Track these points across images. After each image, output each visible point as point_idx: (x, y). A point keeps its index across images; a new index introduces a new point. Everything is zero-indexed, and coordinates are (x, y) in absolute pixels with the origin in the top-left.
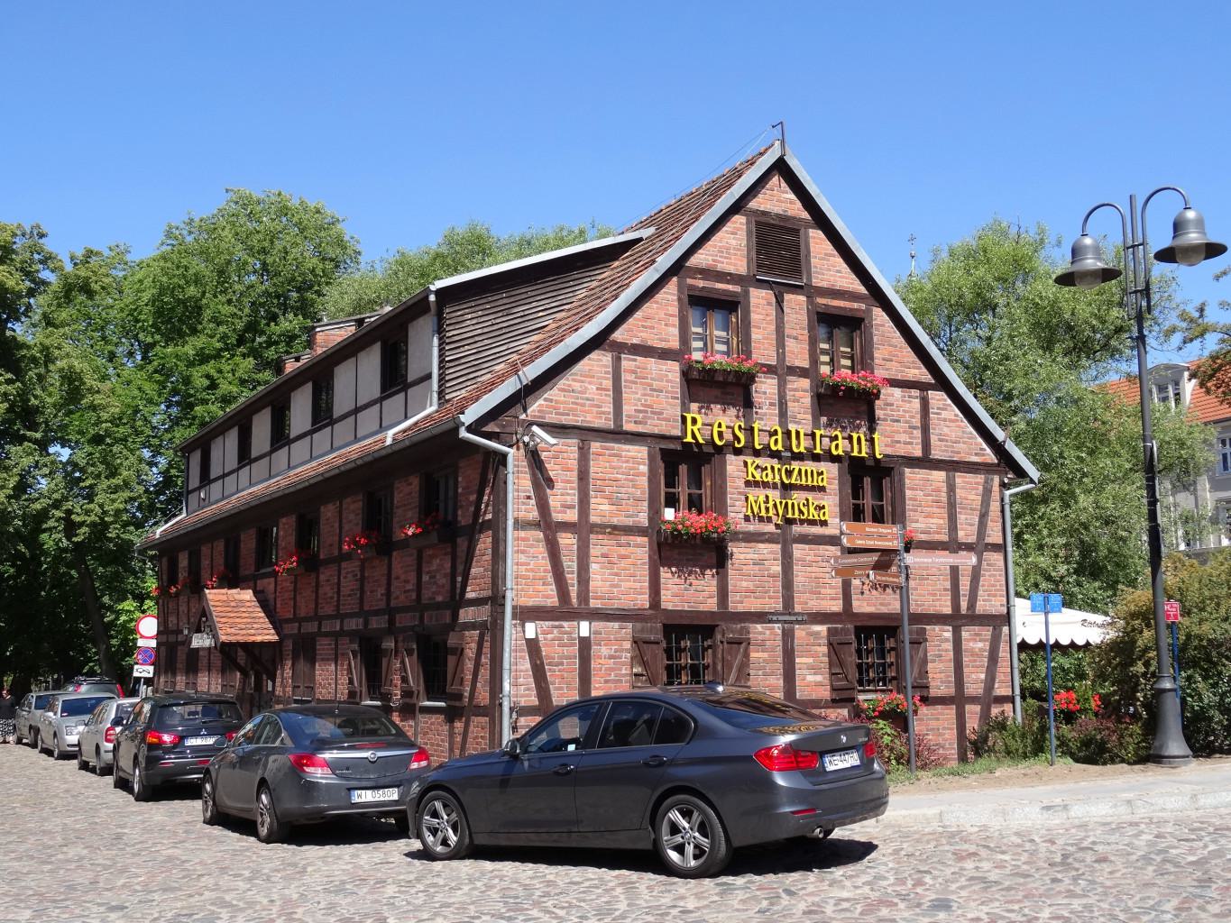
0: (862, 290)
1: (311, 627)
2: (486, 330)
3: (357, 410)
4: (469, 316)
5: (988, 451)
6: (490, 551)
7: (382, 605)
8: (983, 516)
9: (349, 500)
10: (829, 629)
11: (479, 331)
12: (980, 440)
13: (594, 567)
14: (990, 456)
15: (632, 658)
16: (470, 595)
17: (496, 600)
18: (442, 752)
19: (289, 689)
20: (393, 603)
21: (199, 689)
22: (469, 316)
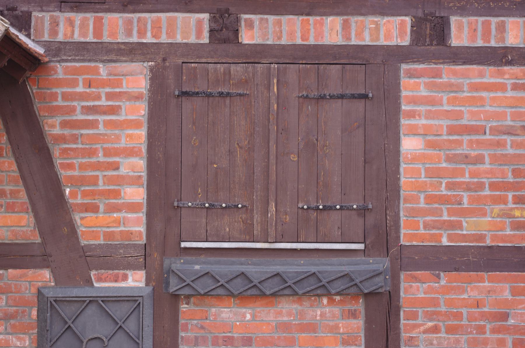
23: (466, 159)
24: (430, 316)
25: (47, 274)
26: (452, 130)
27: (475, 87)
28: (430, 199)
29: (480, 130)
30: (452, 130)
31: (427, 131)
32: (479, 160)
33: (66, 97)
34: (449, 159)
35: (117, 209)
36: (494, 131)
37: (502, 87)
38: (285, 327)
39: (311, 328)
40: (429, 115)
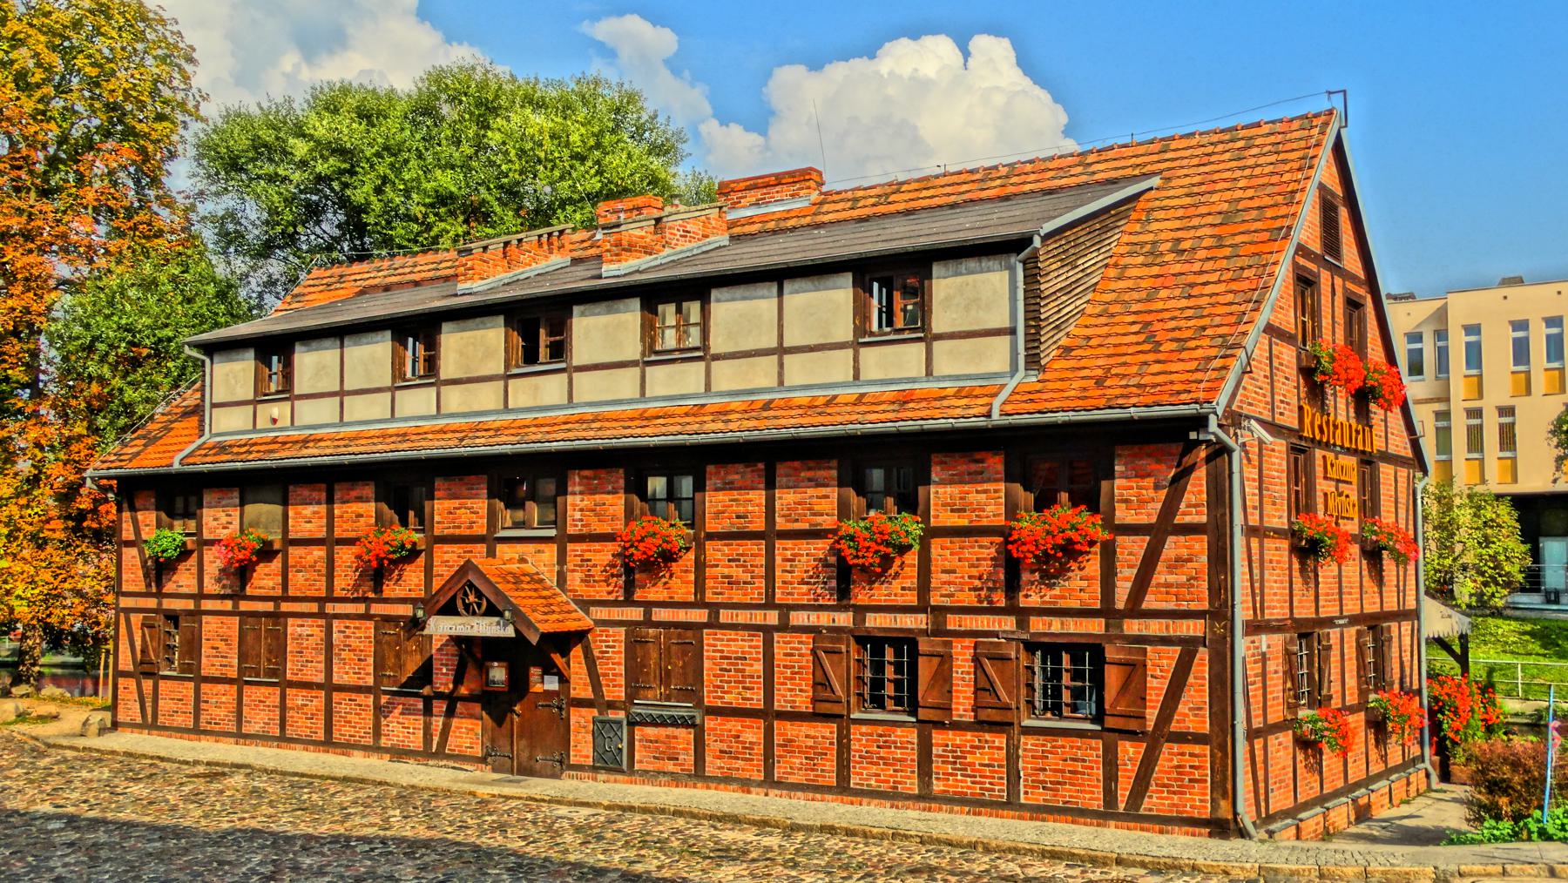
0: (1361, 275)
1: (699, 616)
2: (1063, 285)
3: (781, 351)
4: (1054, 267)
5: (1408, 446)
6: (1204, 559)
7: (912, 599)
8: (1407, 511)
9: (797, 464)
10: (1358, 632)
11: (1059, 286)
12: (1405, 434)
13: (1266, 572)
14: (1408, 452)
15: (1285, 673)
16: (1150, 602)
17: (1220, 611)
18: (1089, 780)
19: (616, 690)
20: (935, 599)
21: (289, 676)
22: (1054, 267)
23: (726, 670)
24: (715, 735)
25: (595, 712)
26: (722, 658)
27: (728, 640)
28: (715, 686)
29: (729, 658)
30: (722, 658)
31: (714, 658)
32: (730, 670)
33: (601, 641)
34: (721, 670)
35: (614, 686)
36: (736, 658)
37: (737, 640)
38: (667, 736)
39: (675, 737)
40: (714, 651)
